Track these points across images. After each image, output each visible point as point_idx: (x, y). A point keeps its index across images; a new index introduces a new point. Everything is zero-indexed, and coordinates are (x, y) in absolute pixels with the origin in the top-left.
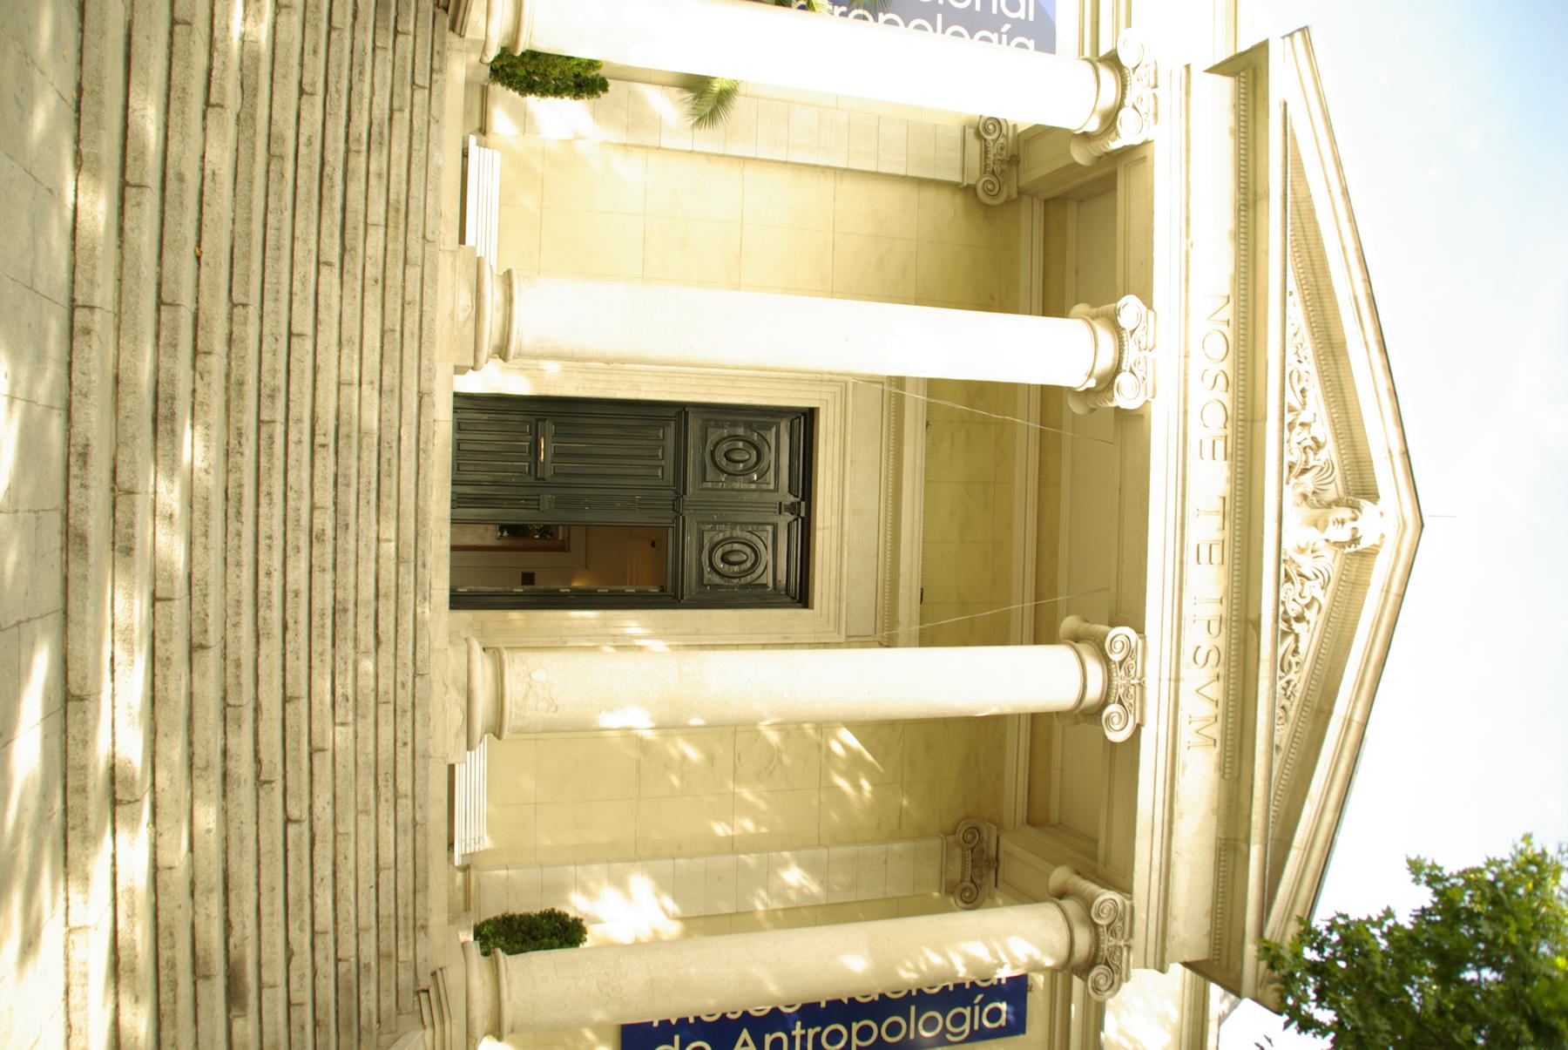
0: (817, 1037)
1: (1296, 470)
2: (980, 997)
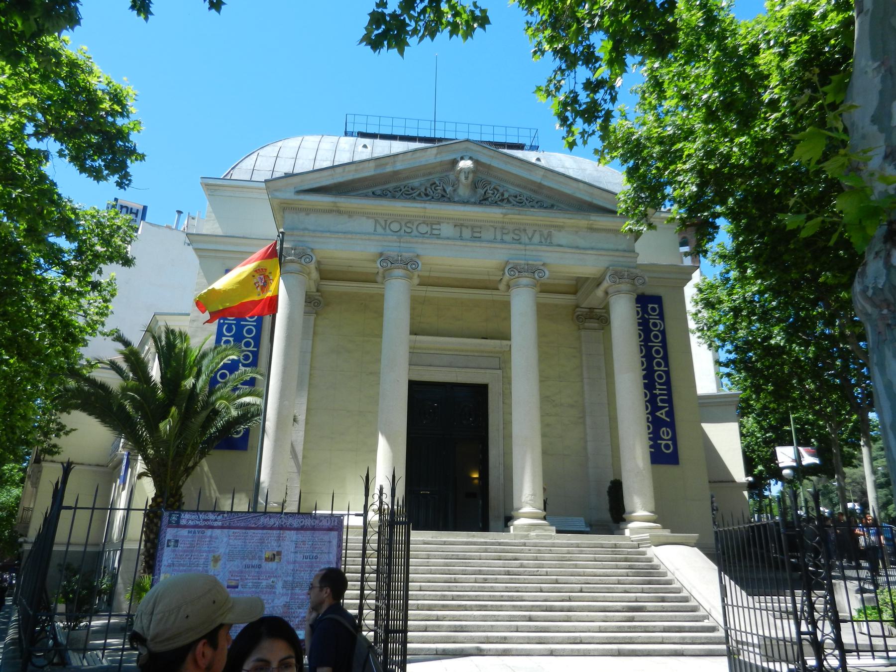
0: (660, 384)
1: (444, 194)
2: (646, 316)
